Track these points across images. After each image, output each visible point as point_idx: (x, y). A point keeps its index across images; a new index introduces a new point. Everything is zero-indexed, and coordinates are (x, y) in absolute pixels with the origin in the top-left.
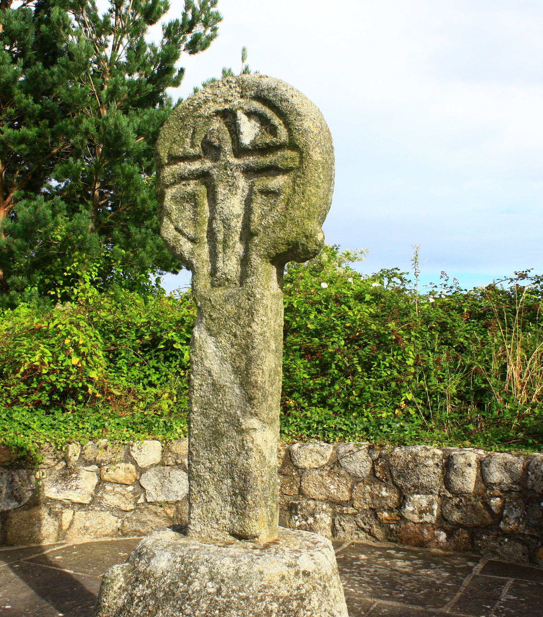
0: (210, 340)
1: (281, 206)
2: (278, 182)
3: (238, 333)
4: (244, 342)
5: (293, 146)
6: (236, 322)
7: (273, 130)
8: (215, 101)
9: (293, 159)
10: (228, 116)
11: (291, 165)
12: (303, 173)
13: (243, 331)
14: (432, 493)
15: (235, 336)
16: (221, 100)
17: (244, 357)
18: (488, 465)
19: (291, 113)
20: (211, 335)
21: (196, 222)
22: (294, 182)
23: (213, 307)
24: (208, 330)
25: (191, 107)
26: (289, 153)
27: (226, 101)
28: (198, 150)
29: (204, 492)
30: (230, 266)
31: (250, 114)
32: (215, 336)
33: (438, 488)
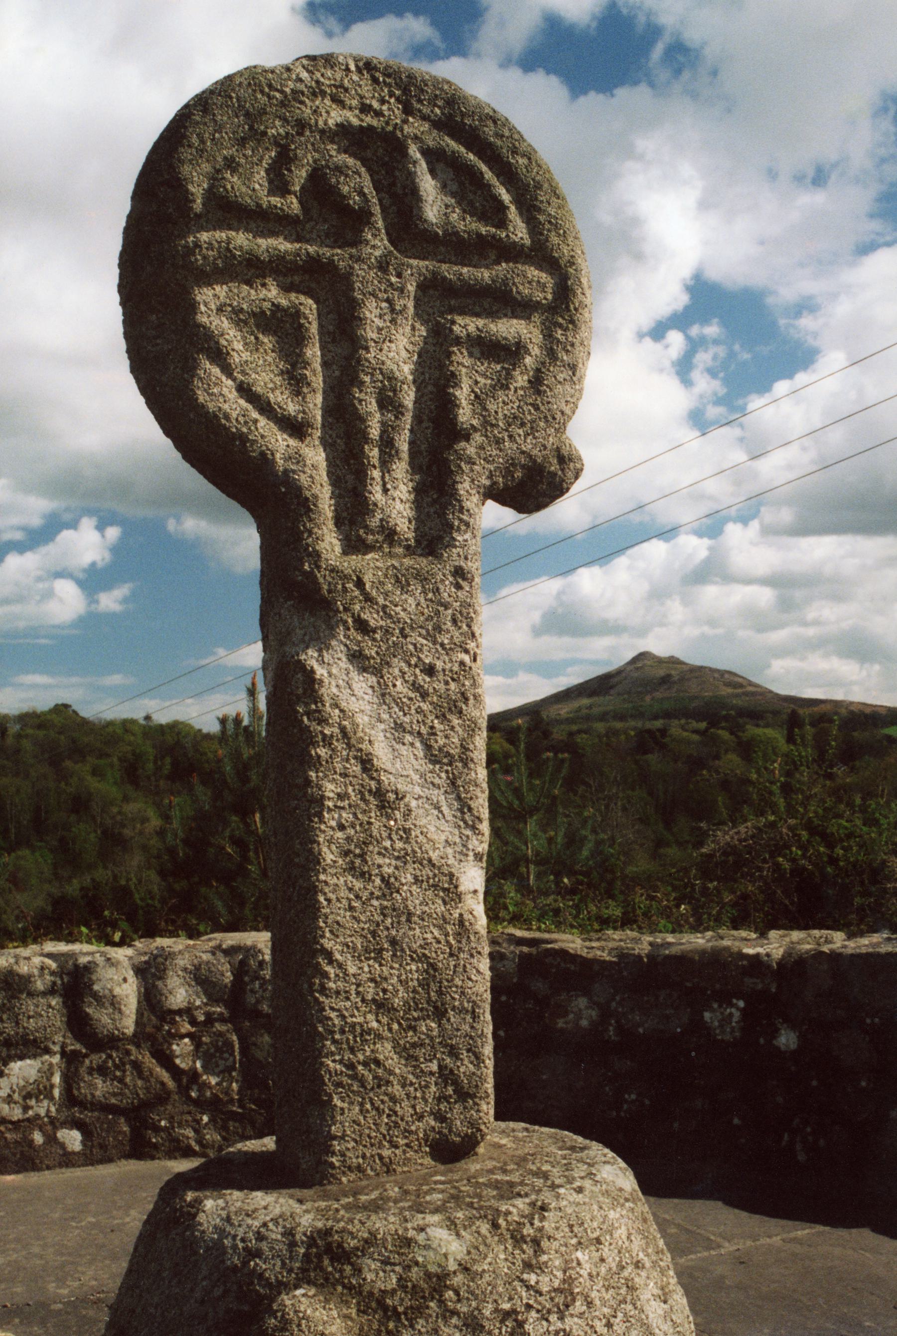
0: (362, 684)
1: (521, 380)
2: (508, 328)
3: (439, 665)
4: (453, 686)
5: (542, 254)
6: (429, 636)
7: (495, 213)
8: (336, 100)
9: (543, 287)
10: (380, 150)
11: (538, 296)
12: (572, 322)
13: (451, 661)
14: (47, 1051)
15: (430, 671)
16: (354, 103)
17: (456, 722)
18: (161, 974)
19: (538, 186)
20: (364, 670)
21: (296, 382)
22: (548, 335)
23: (368, 598)
24: (357, 658)
25: (278, 95)
26: (533, 272)
27: (365, 109)
28: (293, 205)
29: (365, 1064)
30: (395, 500)
31: (434, 157)
32: (377, 672)
33: (58, 1038)
